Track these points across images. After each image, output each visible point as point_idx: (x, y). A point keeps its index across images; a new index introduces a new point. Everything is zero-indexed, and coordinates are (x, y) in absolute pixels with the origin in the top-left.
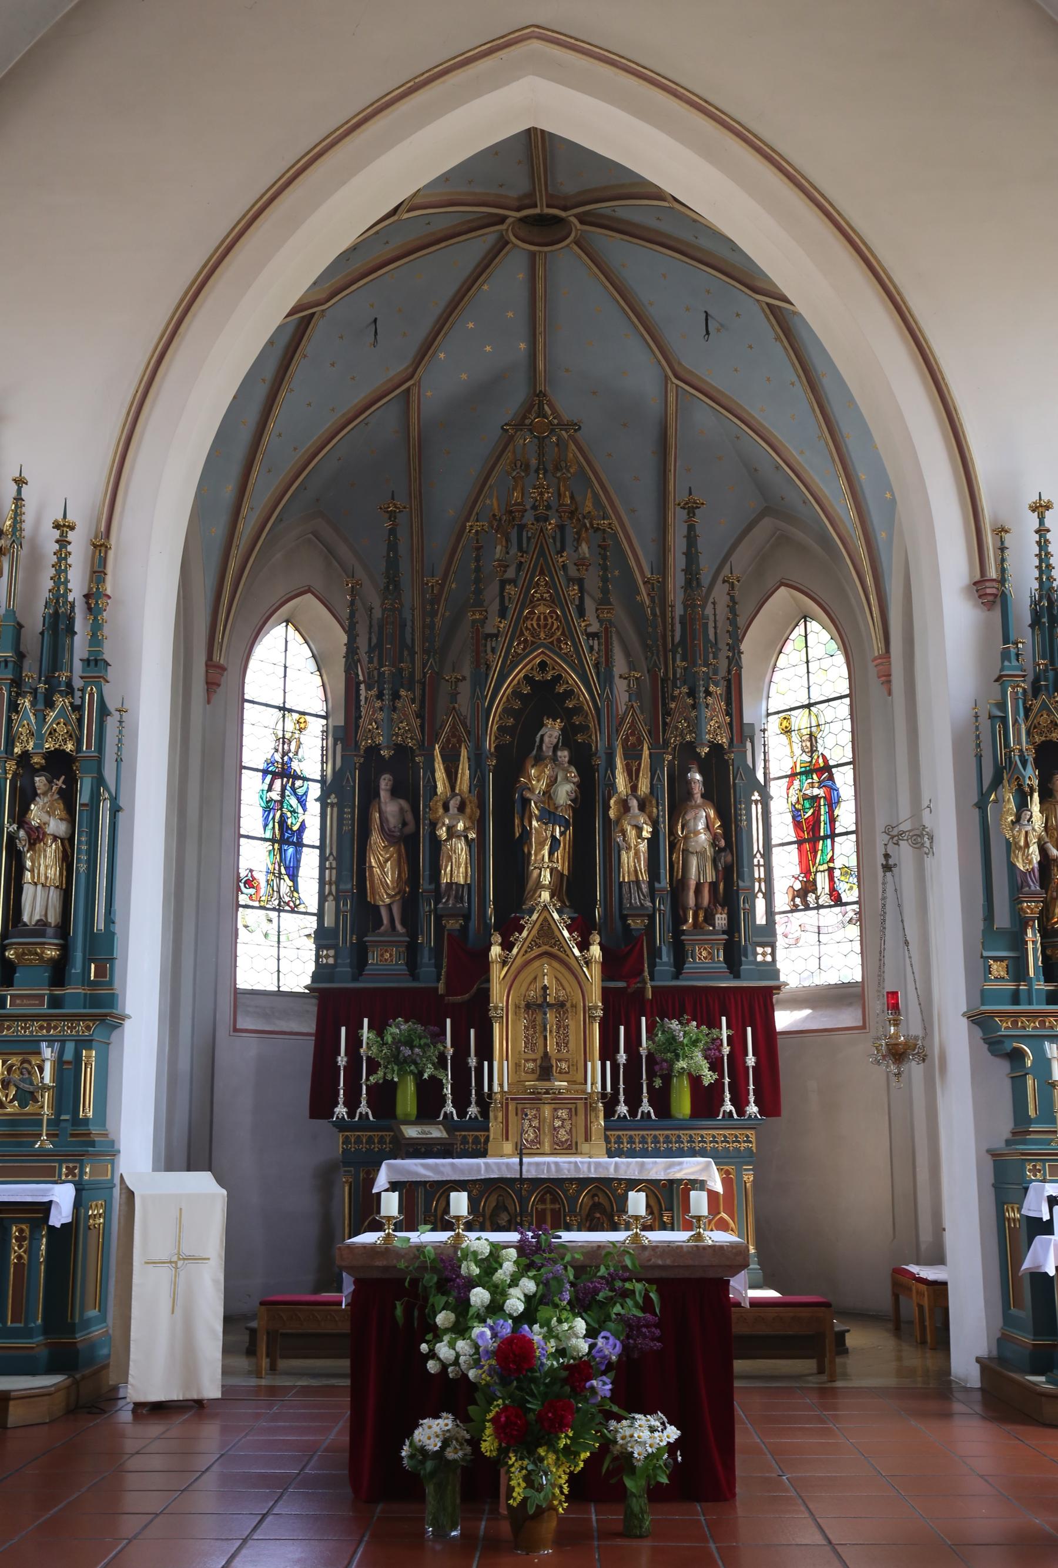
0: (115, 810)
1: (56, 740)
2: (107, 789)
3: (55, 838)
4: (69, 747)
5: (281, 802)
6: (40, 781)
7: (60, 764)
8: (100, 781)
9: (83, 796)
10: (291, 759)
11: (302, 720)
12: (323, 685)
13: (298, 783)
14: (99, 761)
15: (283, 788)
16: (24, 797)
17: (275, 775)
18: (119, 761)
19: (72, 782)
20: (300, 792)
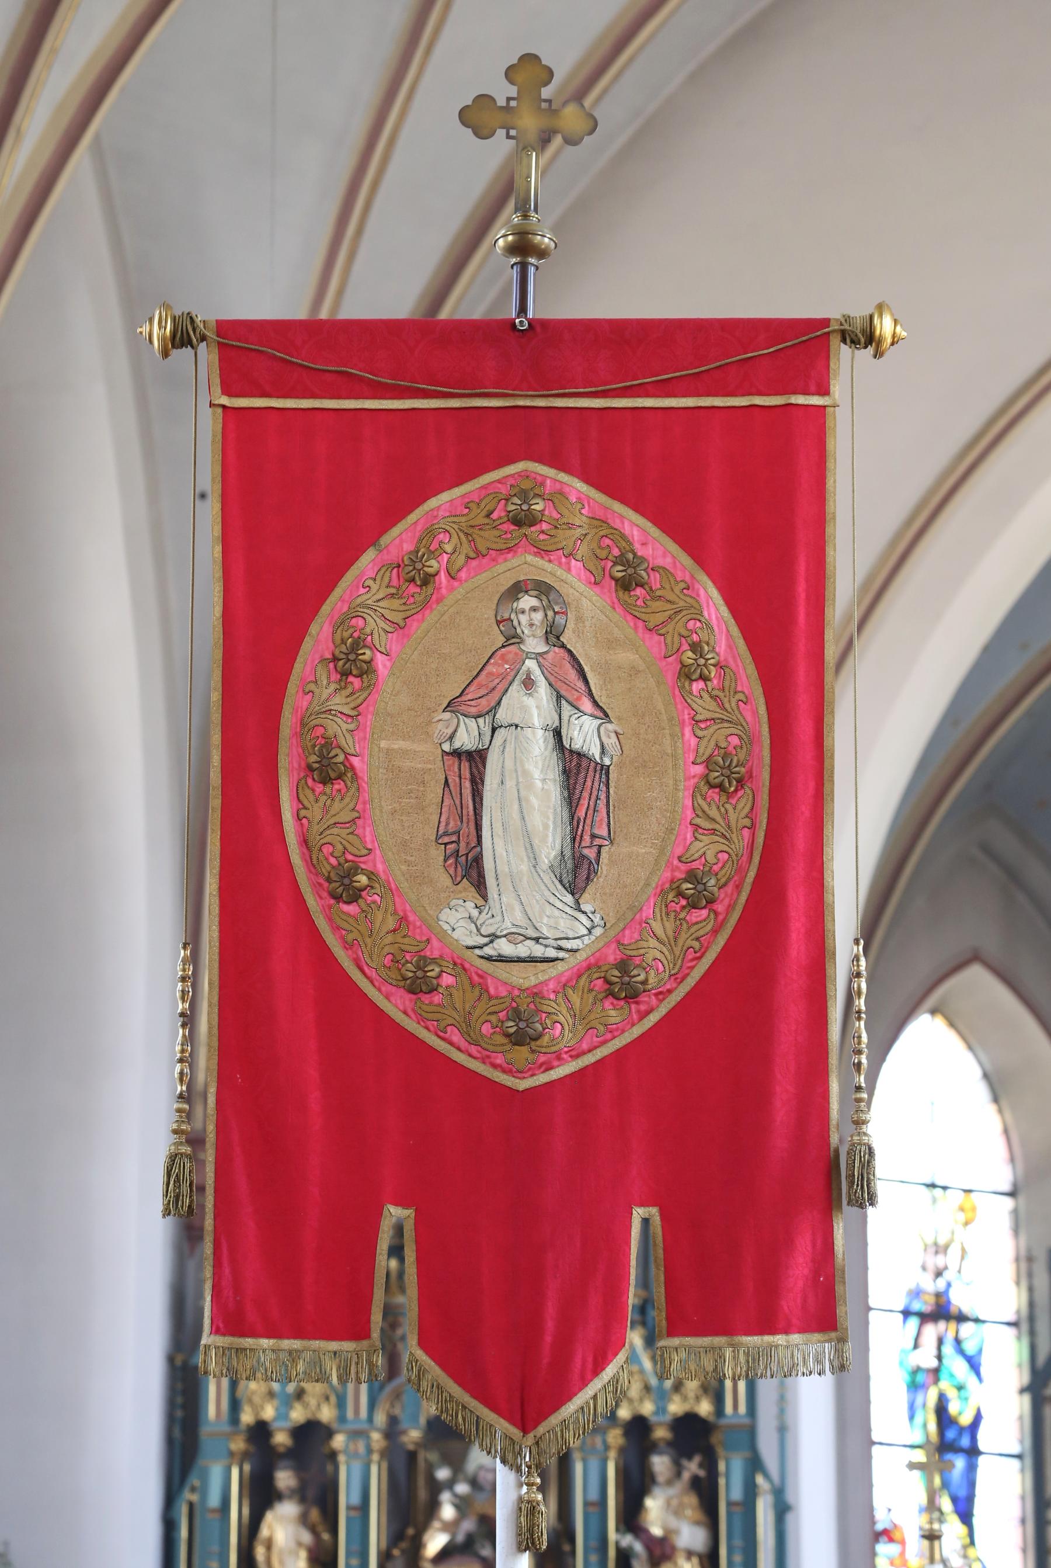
0: (782, 1510)
1: (685, 1399)
2: (767, 1476)
3: (690, 1554)
4: (705, 1408)
5: (936, 1372)
6: (660, 1463)
7: (693, 1436)
8: (755, 1464)
9: (731, 1487)
10: (949, 1285)
11: (967, 1206)
12: (1006, 1131)
13: (967, 1329)
14: (751, 1432)
15: (940, 1342)
16: (635, 1488)
17: (925, 1318)
18: (782, 1430)
19: (710, 1464)
20: (970, 1348)
